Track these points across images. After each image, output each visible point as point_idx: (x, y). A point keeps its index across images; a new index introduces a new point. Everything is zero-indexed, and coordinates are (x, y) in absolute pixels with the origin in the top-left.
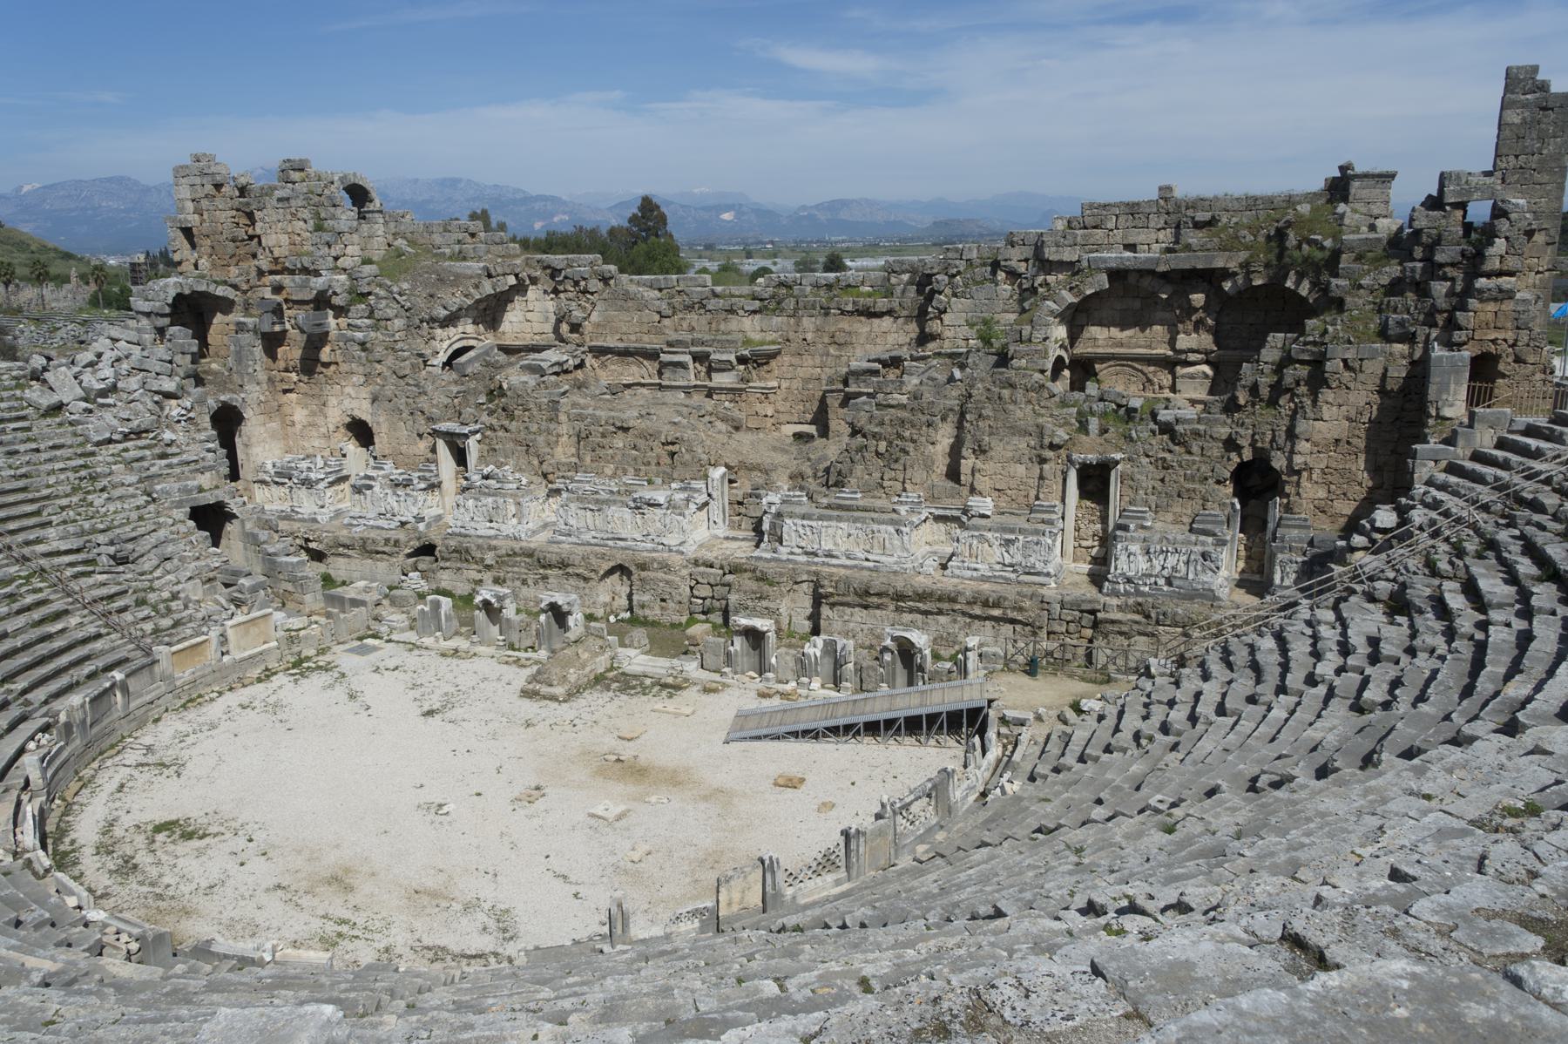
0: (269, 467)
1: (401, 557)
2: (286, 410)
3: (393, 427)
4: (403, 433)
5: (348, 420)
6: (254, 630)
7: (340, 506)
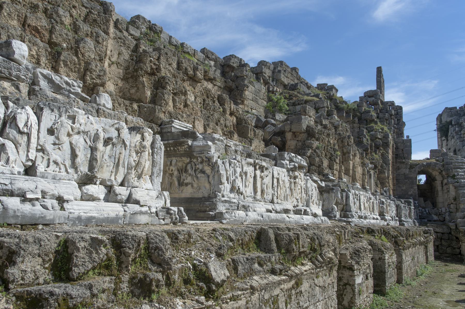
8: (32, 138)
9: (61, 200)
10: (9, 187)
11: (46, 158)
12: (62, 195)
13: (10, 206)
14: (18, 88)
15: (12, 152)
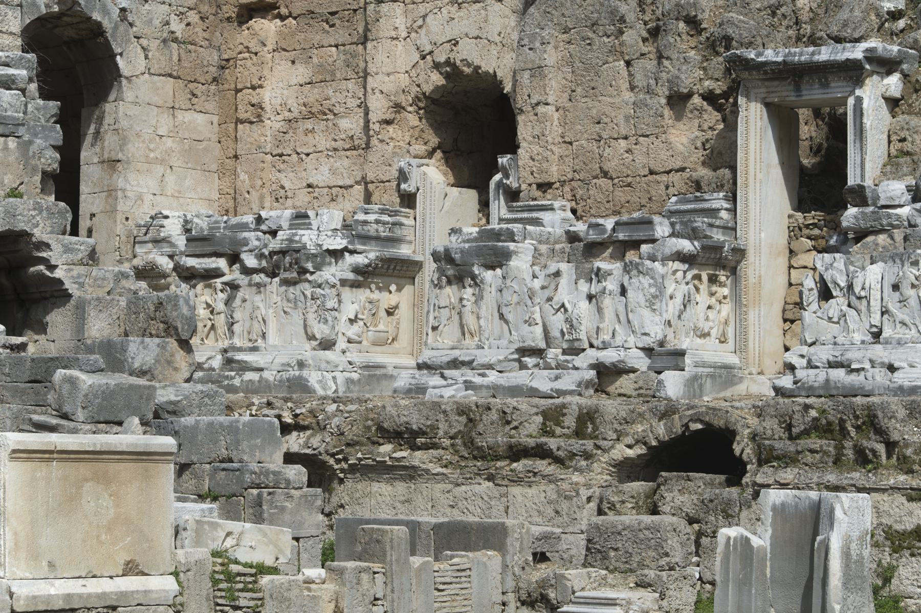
0: (173, 229)
1: (600, 474)
2: (245, 72)
3: (585, 81)
4: (619, 101)
5: (437, 79)
6: (97, 502)
7: (379, 357)
8: (872, 303)
9: (892, 368)
10: (839, 359)
11: (892, 320)
12: (892, 362)
13: (831, 378)
14: (892, 238)
15: (855, 321)
